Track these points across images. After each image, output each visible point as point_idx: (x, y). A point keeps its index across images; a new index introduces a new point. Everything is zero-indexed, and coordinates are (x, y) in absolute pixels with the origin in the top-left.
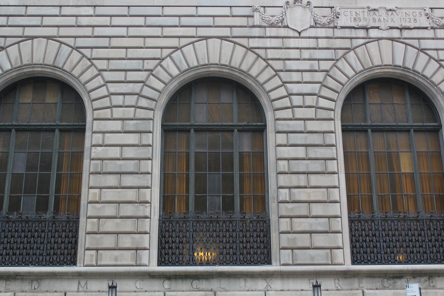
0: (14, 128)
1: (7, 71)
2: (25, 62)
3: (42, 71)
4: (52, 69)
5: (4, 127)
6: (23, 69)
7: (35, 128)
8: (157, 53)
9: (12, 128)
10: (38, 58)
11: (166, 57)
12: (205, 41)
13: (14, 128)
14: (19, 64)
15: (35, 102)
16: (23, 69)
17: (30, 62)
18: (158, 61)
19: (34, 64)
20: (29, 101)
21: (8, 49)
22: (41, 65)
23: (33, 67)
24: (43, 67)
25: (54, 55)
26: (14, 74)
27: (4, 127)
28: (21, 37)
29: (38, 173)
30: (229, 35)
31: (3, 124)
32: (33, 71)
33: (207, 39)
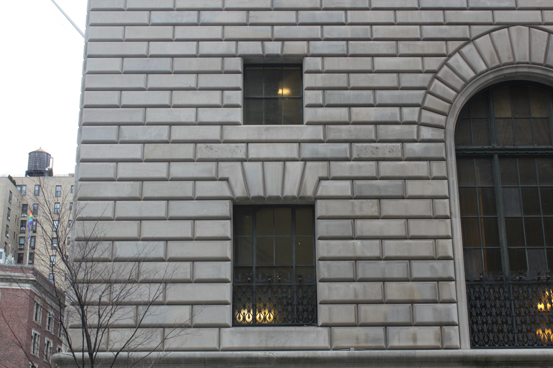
0: (498, 154)
1: (482, 73)
2: (505, 60)
3: (529, 73)
4: (543, 69)
5: (483, 152)
6: (503, 69)
7: (527, 153)
8: (440, 47)
9: (494, 154)
10: (522, 55)
11: (454, 53)
12: (506, 30)
13: (498, 154)
14: (498, 63)
15: (517, 116)
16: (503, 69)
17: (511, 60)
18: (444, 58)
19: (518, 63)
20: (509, 114)
21: (477, 41)
22: (528, 63)
23: (516, 67)
24: (530, 67)
25: (544, 49)
26: (491, 76)
27: (483, 152)
28: (491, 24)
29: (542, 216)
30: (540, 20)
31: (480, 147)
32: (516, 73)
33: (508, 27)
